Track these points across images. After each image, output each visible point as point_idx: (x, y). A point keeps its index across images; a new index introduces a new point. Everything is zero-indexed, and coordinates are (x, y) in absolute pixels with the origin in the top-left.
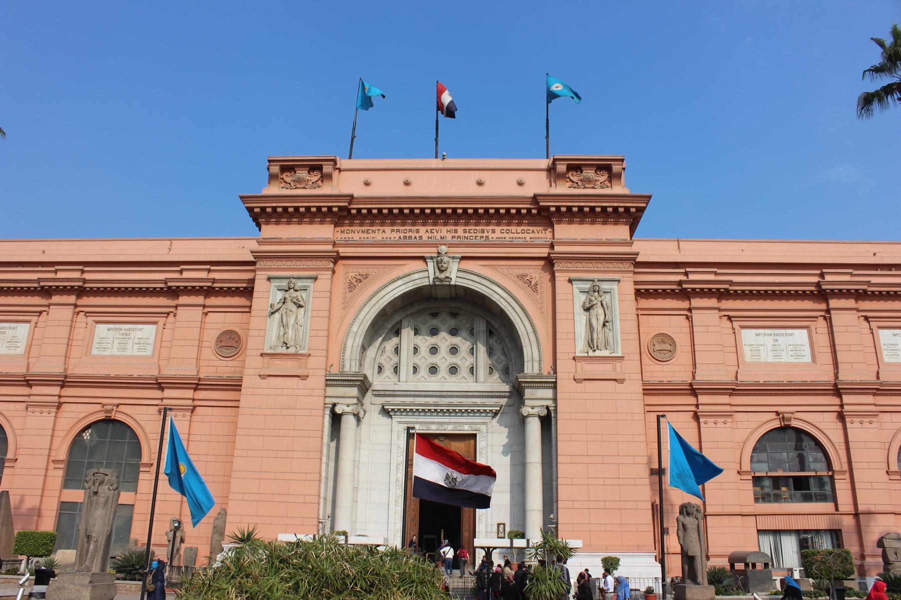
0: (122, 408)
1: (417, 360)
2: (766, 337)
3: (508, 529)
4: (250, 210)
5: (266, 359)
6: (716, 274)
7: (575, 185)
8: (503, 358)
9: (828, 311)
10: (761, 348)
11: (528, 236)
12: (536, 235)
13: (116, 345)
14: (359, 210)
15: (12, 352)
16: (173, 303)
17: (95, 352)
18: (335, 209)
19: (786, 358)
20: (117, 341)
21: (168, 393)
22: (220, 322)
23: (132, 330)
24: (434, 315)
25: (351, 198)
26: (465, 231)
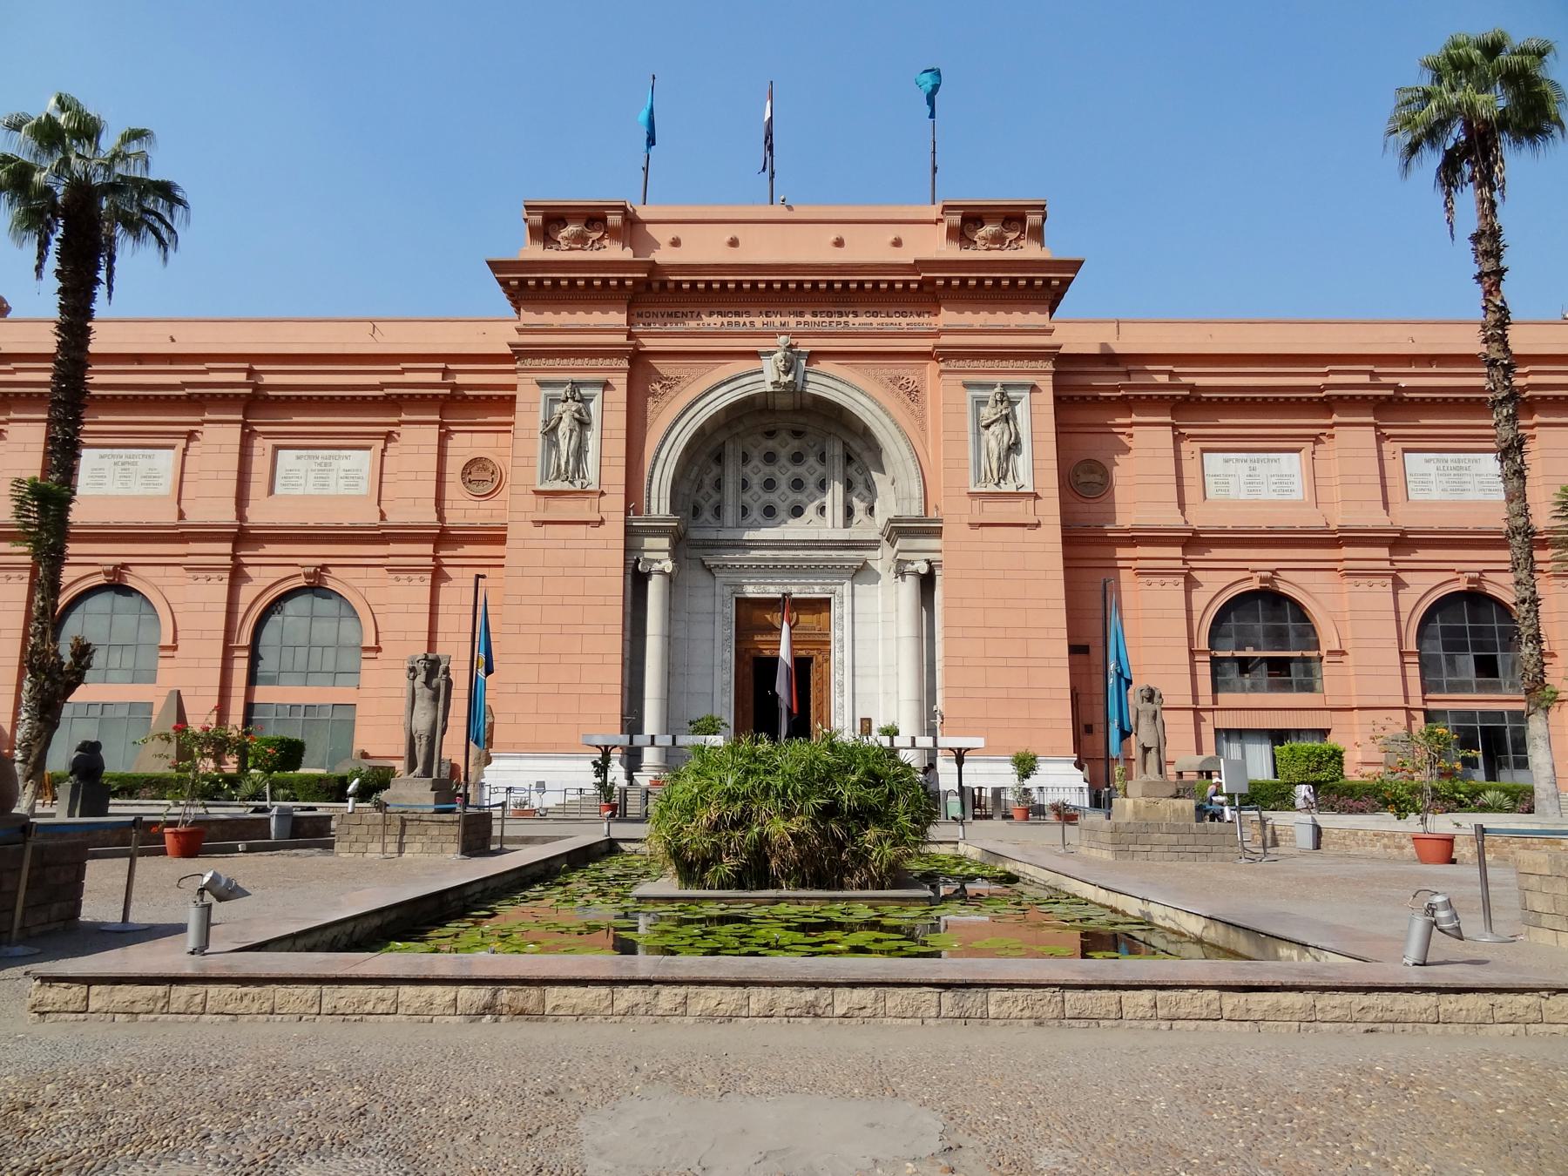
1: (746, 497)
2: (1240, 465)
3: (875, 727)
4: (504, 283)
5: (541, 499)
8: (866, 493)
10: (1231, 480)
11: (904, 321)
12: (915, 319)
13: (311, 480)
14: (664, 284)
15: (151, 492)
16: (395, 420)
18: (629, 283)
19: (1267, 494)
20: (313, 474)
22: (464, 446)
23: (334, 457)
24: (770, 434)
25: (653, 267)
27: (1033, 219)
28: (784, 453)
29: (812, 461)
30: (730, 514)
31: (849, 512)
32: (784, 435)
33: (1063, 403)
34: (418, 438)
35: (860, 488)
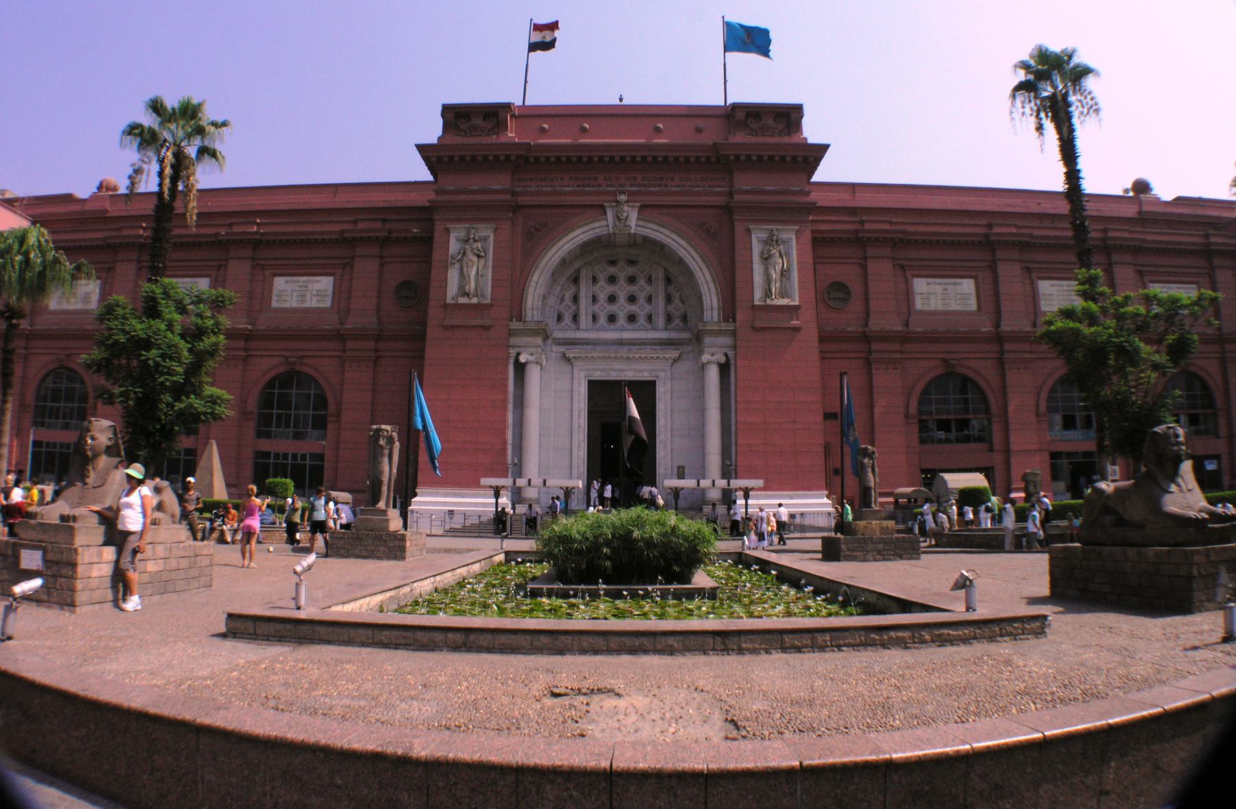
0: (306, 361)
1: (596, 308)
6: (891, 223)
7: (753, 132)
8: (681, 305)
9: (994, 262)
14: (537, 159)
17: (274, 304)
19: (954, 306)
20: (295, 294)
21: (350, 344)
24: (613, 263)
26: (644, 179)
27: (794, 116)
28: (622, 277)
29: (642, 282)
30: (584, 320)
31: (669, 318)
32: (622, 264)
33: (815, 241)
34: (366, 268)
35: (677, 302)
